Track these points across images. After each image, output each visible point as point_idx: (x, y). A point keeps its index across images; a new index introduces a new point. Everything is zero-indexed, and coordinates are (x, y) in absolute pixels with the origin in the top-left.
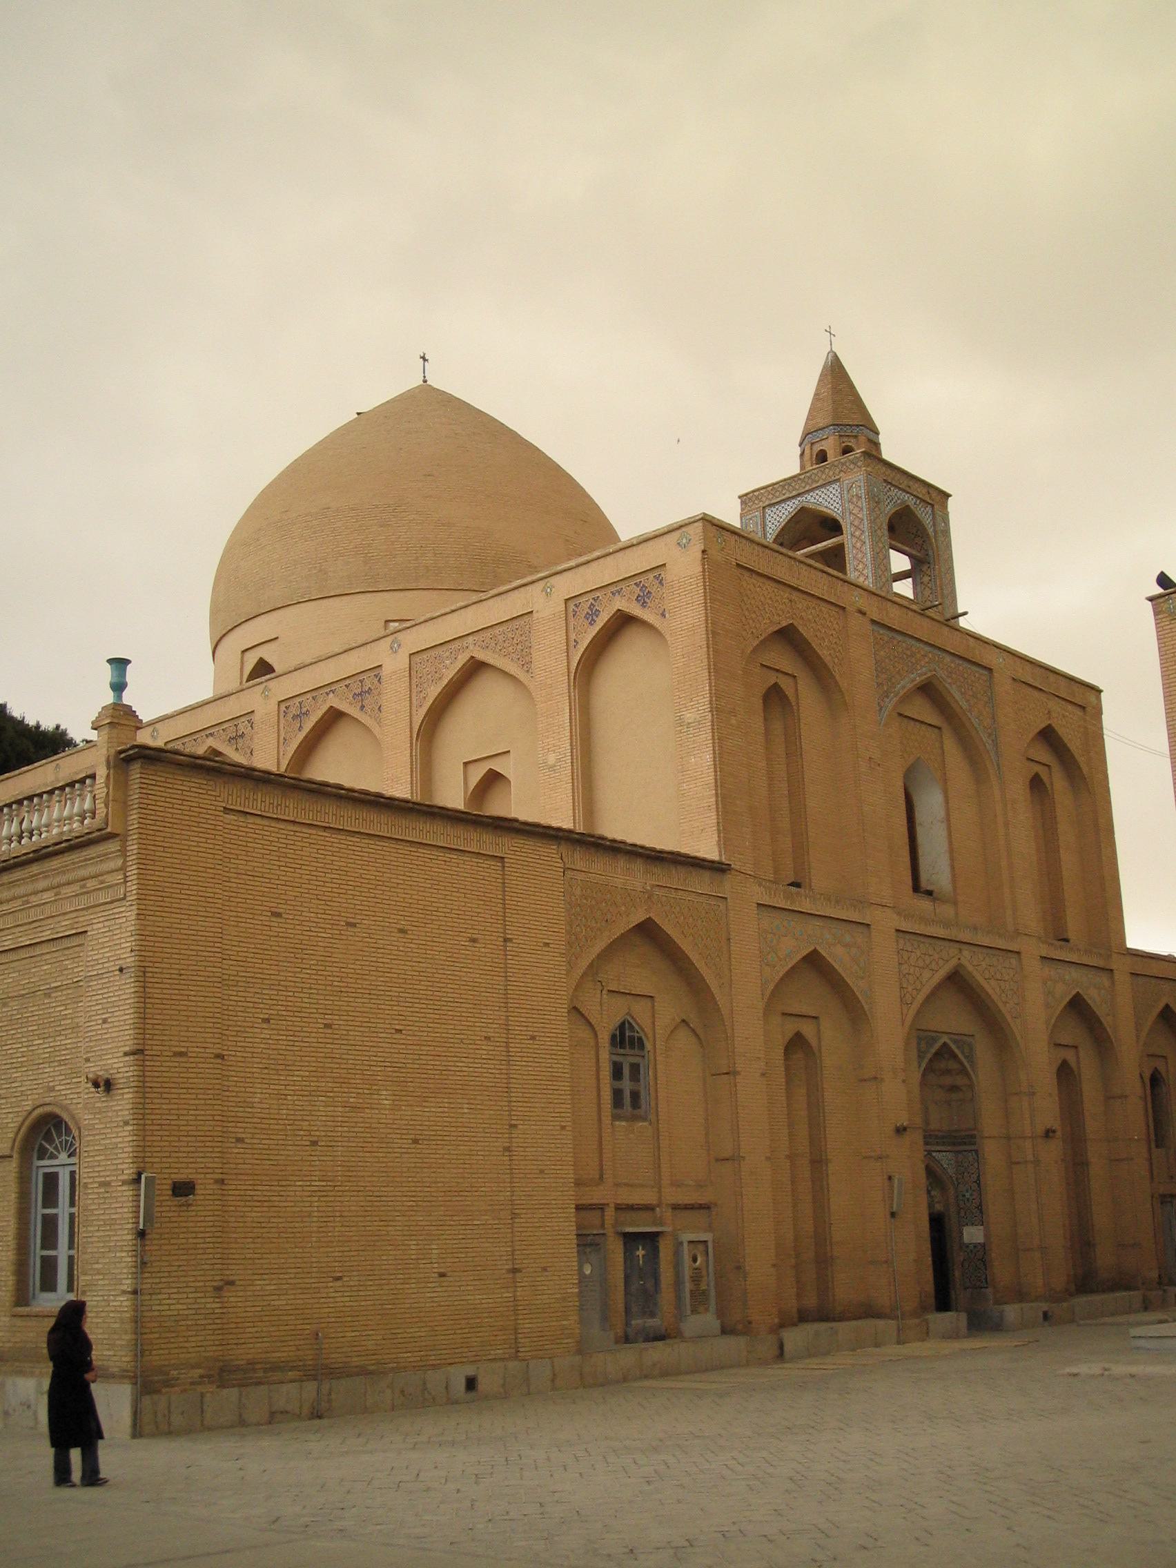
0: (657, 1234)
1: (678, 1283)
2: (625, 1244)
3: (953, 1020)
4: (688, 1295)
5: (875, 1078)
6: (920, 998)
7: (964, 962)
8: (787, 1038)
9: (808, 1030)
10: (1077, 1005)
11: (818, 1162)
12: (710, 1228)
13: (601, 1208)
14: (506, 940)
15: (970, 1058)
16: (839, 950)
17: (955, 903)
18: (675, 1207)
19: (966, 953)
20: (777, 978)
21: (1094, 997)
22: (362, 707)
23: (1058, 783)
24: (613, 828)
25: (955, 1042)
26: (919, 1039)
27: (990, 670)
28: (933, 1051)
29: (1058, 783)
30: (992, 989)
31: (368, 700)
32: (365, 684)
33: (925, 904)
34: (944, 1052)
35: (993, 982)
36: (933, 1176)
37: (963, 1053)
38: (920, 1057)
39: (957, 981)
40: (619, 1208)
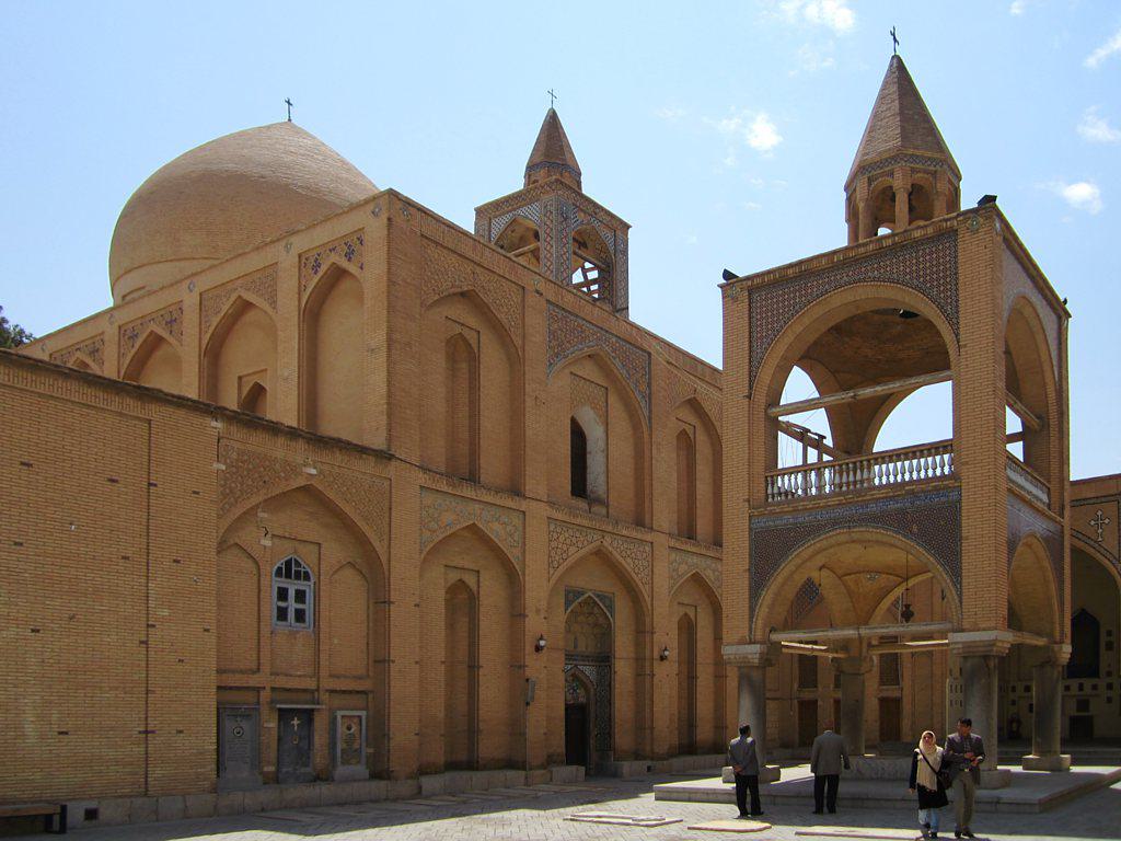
0: (313, 710)
1: (332, 744)
2: (279, 716)
3: (595, 582)
4: (339, 754)
5: (520, 615)
6: (565, 565)
7: (605, 544)
8: (449, 584)
9: (470, 580)
10: (697, 579)
11: (473, 666)
12: (366, 708)
13: (258, 690)
14: (150, 484)
15: (611, 608)
16: (496, 526)
17: (607, 507)
18: (332, 691)
19: (608, 539)
20: (436, 540)
21: (709, 576)
22: (171, 332)
23: (701, 439)
24: (329, 428)
25: (598, 596)
26: (567, 592)
27: (650, 354)
28: (580, 600)
29: (701, 439)
30: (628, 565)
31: (175, 327)
32: (172, 320)
33: (582, 504)
34: (590, 602)
35: (629, 560)
36: (575, 679)
37: (603, 603)
38: (568, 603)
39: (601, 555)
40: (273, 689)
